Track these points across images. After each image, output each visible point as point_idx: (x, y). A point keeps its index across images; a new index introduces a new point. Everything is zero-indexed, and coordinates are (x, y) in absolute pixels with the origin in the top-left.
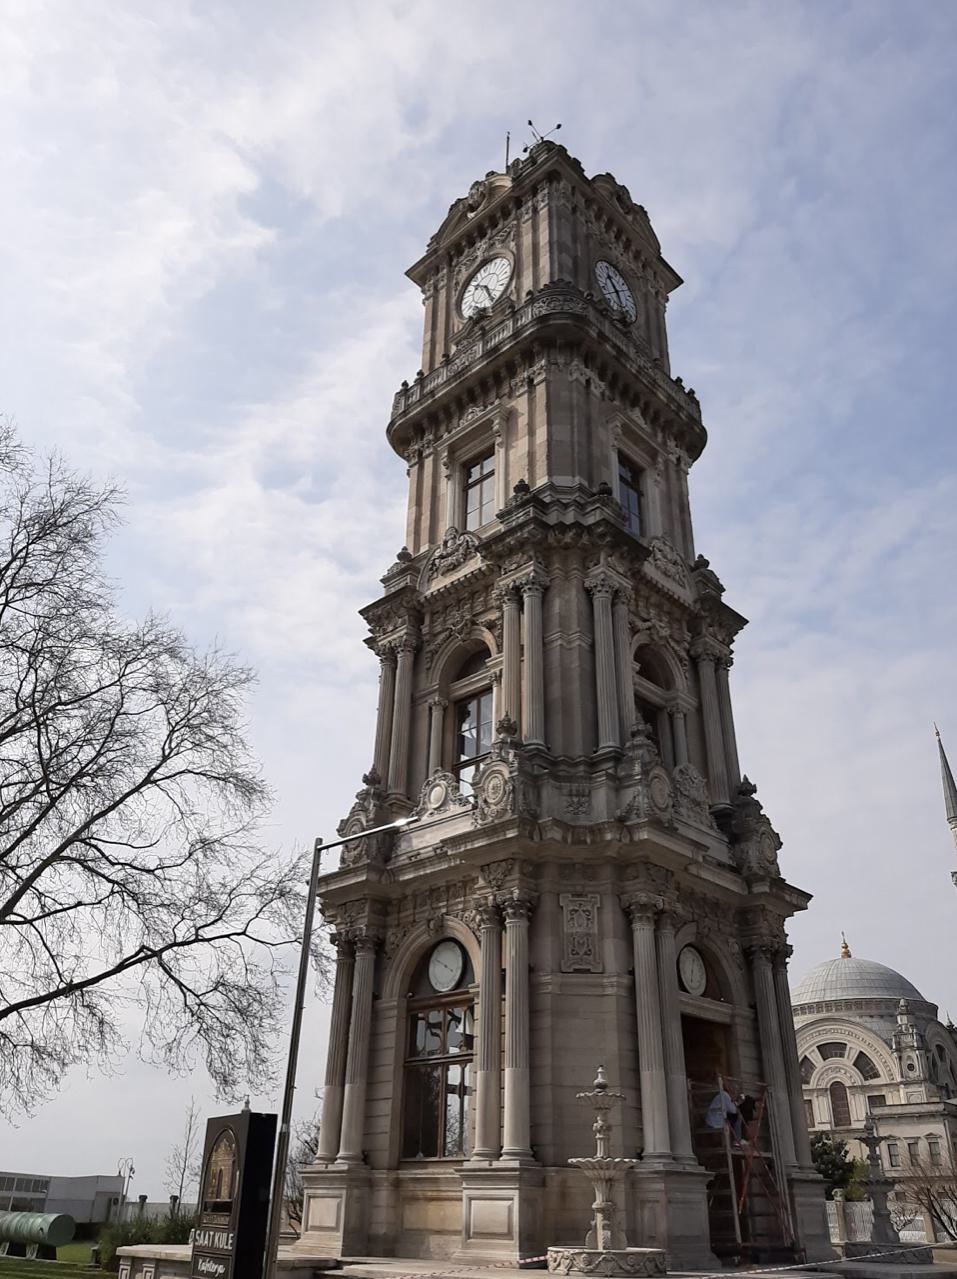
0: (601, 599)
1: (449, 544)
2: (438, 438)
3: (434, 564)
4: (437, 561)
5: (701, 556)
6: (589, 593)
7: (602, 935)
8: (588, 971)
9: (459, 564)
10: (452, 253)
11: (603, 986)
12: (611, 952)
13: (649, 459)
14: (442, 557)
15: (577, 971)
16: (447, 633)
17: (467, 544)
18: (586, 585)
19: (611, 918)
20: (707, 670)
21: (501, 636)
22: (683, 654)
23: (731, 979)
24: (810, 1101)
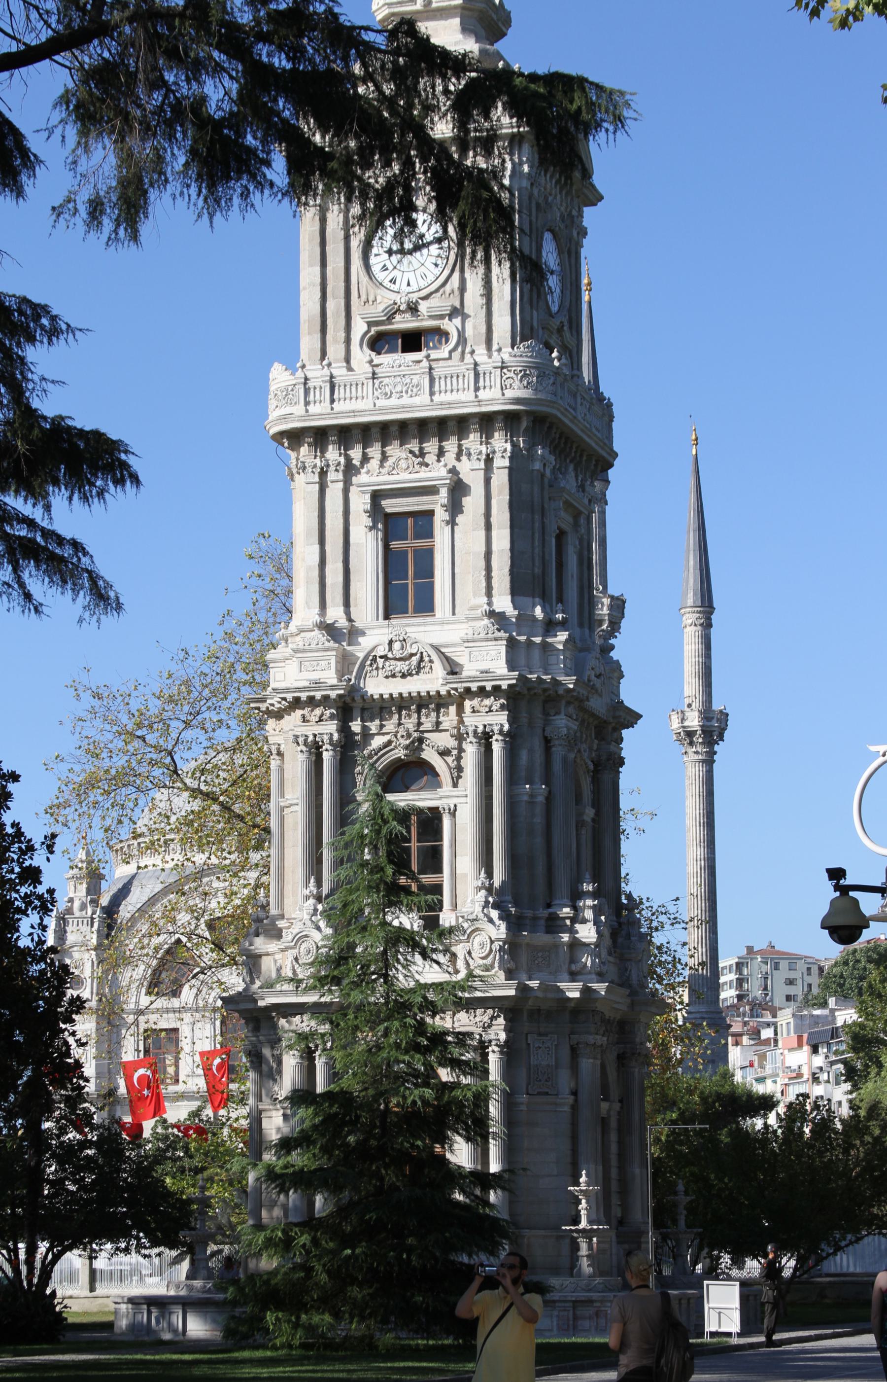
0: (558, 751)
1: (397, 646)
2: (350, 470)
3: (374, 659)
4: (380, 662)
6: (547, 741)
8: (547, 1094)
9: (411, 675)
12: (564, 1081)
13: (571, 520)
15: (539, 1094)
16: (385, 739)
17: (422, 657)
18: (547, 734)
19: (565, 1053)
20: (606, 777)
21: (460, 769)
22: (592, 767)
24: (176, 1030)
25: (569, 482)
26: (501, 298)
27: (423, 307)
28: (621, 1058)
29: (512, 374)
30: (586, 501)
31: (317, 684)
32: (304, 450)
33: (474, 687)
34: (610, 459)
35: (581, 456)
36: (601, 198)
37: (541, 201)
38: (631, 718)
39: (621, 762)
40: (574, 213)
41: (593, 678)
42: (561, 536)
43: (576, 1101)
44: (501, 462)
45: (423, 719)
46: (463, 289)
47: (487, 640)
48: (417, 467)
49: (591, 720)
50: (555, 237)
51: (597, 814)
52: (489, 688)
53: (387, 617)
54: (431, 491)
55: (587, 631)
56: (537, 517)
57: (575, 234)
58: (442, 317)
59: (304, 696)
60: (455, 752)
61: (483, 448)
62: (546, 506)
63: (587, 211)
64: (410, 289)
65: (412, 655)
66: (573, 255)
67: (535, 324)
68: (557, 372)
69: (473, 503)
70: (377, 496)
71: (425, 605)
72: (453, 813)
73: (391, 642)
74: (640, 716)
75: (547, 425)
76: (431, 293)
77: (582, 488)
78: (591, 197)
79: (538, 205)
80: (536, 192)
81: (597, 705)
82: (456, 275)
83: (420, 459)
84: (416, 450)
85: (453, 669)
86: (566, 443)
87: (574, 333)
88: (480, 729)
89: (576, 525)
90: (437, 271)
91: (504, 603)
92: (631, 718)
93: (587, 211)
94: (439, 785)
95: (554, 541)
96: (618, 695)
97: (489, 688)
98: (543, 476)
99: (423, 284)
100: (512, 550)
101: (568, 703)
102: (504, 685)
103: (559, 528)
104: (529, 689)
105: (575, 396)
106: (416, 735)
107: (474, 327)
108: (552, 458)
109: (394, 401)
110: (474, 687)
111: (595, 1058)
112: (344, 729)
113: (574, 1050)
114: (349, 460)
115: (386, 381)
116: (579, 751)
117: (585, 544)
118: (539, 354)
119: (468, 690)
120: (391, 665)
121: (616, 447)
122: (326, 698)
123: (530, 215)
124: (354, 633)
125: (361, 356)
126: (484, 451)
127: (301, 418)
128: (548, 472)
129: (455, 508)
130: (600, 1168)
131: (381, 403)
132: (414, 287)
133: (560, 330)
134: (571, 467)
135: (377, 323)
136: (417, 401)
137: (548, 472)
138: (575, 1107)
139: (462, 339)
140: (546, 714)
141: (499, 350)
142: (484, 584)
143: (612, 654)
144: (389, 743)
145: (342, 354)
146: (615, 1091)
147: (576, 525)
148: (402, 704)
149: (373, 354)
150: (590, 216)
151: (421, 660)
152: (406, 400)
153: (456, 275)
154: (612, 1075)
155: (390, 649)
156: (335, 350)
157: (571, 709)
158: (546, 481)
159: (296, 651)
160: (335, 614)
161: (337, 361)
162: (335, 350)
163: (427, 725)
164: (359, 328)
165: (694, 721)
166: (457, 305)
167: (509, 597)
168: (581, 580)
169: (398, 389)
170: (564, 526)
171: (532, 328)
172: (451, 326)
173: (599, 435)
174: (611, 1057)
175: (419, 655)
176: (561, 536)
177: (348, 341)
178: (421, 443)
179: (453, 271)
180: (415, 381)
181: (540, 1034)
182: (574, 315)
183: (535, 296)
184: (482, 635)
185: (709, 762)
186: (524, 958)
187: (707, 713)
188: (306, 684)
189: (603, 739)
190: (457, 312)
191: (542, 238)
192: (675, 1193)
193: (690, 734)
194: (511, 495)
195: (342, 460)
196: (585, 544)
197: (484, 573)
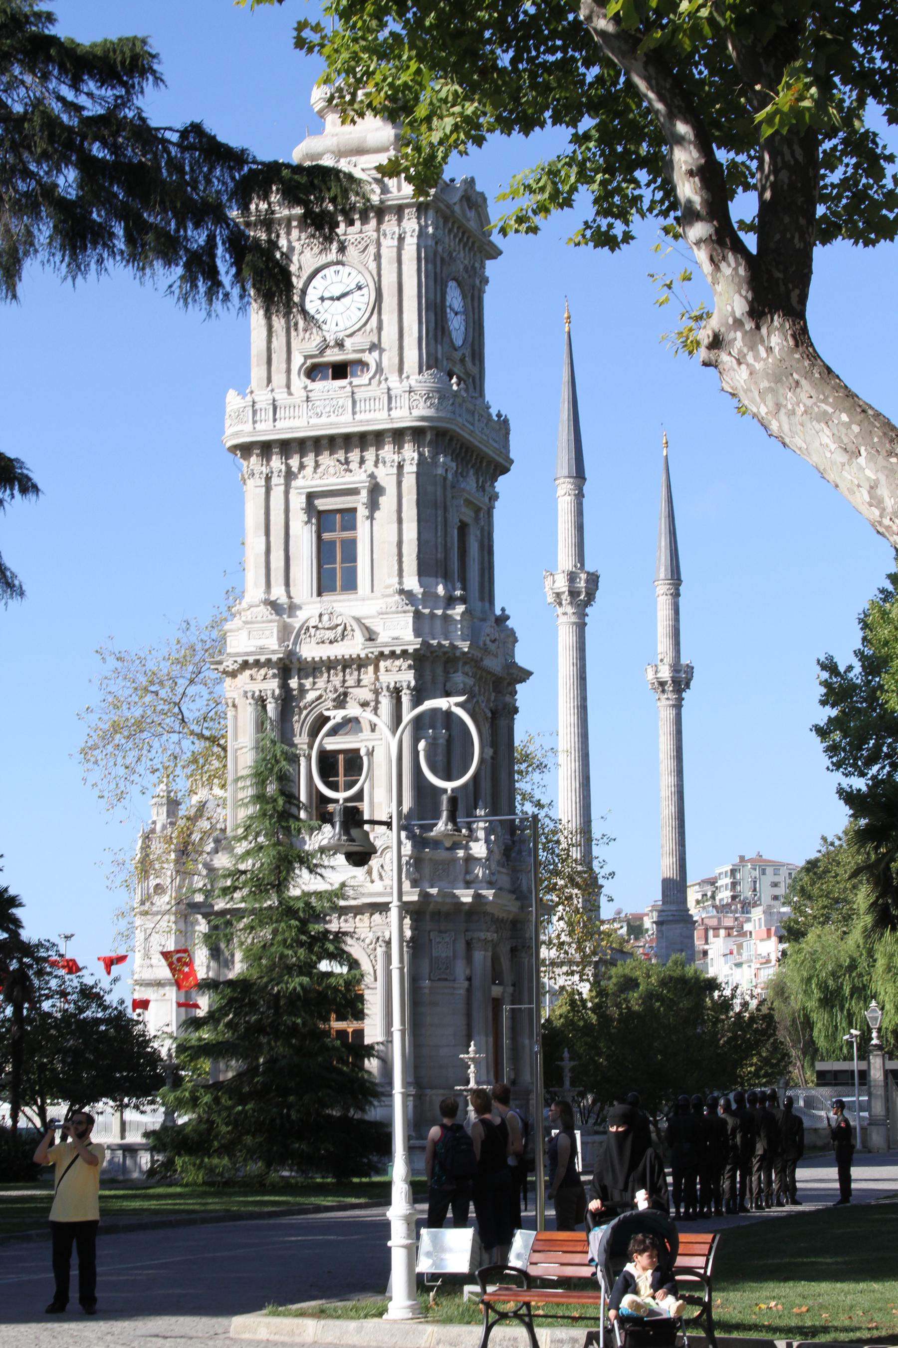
1: (325, 618)
2: (289, 476)
3: (308, 629)
4: (312, 631)
5: (503, 610)
7: (455, 957)
8: (446, 980)
9: (336, 641)
10: (294, 223)
11: (454, 988)
13: (472, 514)
14: (316, 627)
15: (439, 980)
16: (317, 693)
18: (447, 688)
19: (461, 946)
20: (502, 722)
22: (489, 715)
23: (504, 968)
25: (470, 484)
26: (410, 335)
27: (348, 343)
28: (514, 951)
29: (418, 397)
30: (487, 500)
31: (262, 649)
32: (253, 459)
33: (387, 651)
34: (507, 465)
35: (481, 462)
36: (500, 253)
37: (445, 255)
38: (524, 675)
39: (516, 711)
40: (477, 265)
41: (488, 642)
42: (463, 528)
43: (470, 985)
44: (410, 469)
45: (347, 677)
46: (380, 328)
47: (397, 613)
48: (343, 473)
49: (489, 677)
50: (459, 284)
51: (495, 753)
52: (398, 652)
53: (319, 594)
54: (354, 492)
55: (487, 605)
56: (440, 512)
57: (477, 282)
58: (363, 351)
59: (251, 659)
60: (373, 704)
61: (396, 457)
62: (448, 503)
63: (489, 263)
64: (338, 329)
65: (337, 625)
66: (476, 300)
67: (440, 355)
68: (456, 395)
69: (387, 502)
70: (311, 497)
71: (350, 585)
72: (370, 754)
73: (321, 615)
74: (530, 674)
75: (448, 438)
76: (355, 332)
77: (483, 488)
78: (491, 252)
79: (443, 260)
80: (440, 249)
81: (493, 664)
82: (375, 317)
83: (345, 467)
84: (342, 459)
85: (371, 637)
86: (466, 452)
87: (477, 363)
88: (392, 685)
89: (477, 518)
90: (360, 314)
91: (412, 583)
92: (524, 675)
93: (489, 263)
94: (361, 730)
95: (456, 532)
96: (513, 657)
97: (398, 652)
98: (445, 479)
99: (348, 324)
100: (419, 539)
101: (465, 664)
102: (411, 649)
103: (461, 521)
104: (432, 653)
105: (473, 414)
106: (341, 690)
107: (389, 359)
108: (454, 465)
109: (324, 420)
110: (387, 651)
111: (486, 950)
112: (284, 686)
113: (469, 944)
114: (288, 468)
115: (318, 403)
116: (477, 702)
117: (486, 534)
118: (440, 381)
119: (382, 654)
120: (321, 634)
121: (512, 455)
122: (269, 661)
123: (435, 268)
124: (293, 608)
125: (299, 382)
126: (396, 460)
127: (250, 434)
128: (450, 476)
129: (373, 505)
130: (491, 1040)
131: (312, 421)
132: (341, 327)
133: (462, 361)
134: (471, 472)
135: (312, 357)
136: (342, 419)
137: (450, 476)
138: (469, 991)
139: (379, 369)
140: (447, 672)
141: (408, 377)
142: (396, 567)
143: (508, 623)
144: (320, 697)
145: (284, 381)
146: (508, 977)
147: (477, 518)
148: (330, 665)
149: (308, 382)
150: (491, 267)
151: (345, 629)
152: (333, 419)
153: (375, 317)
154: (505, 963)
155: (320, 621)
156: (279, 378)
157: (467, 668)
158: (449, 483)
159: (246, 623)
160: (278, 593)
161: (279, 387)
162: (279, 378)
163: (351, 681)
164: (298, 360)
165: (665, 673)
166: (376, 341)
167: (416, 578)
168: (482, 563)
169: (328, 409)
170: (466, 519)
171: (436, 359)
172: (371, 358)
173: (495, 445)
174: (504, 951)
175: (342, 626)
176: (463, 528)
177: (288, 371)
178: (346, 453)
179: (372, 313)
180: (340, 404)
181: (440, 932)
182: (476, 348)
183: (439, 333)
184: (394, 609)
185: (678, 706)
186: (427, 870)
187: (676, 667)
188: (253, 649)
189: (500, 692)
190: (373, 347)
191: (446, 286)
192: (562, 1059)
193: (662, 684)
194: (418, 494)
195: (283, 468)
196: (486, 534)
197: (396, 558)
